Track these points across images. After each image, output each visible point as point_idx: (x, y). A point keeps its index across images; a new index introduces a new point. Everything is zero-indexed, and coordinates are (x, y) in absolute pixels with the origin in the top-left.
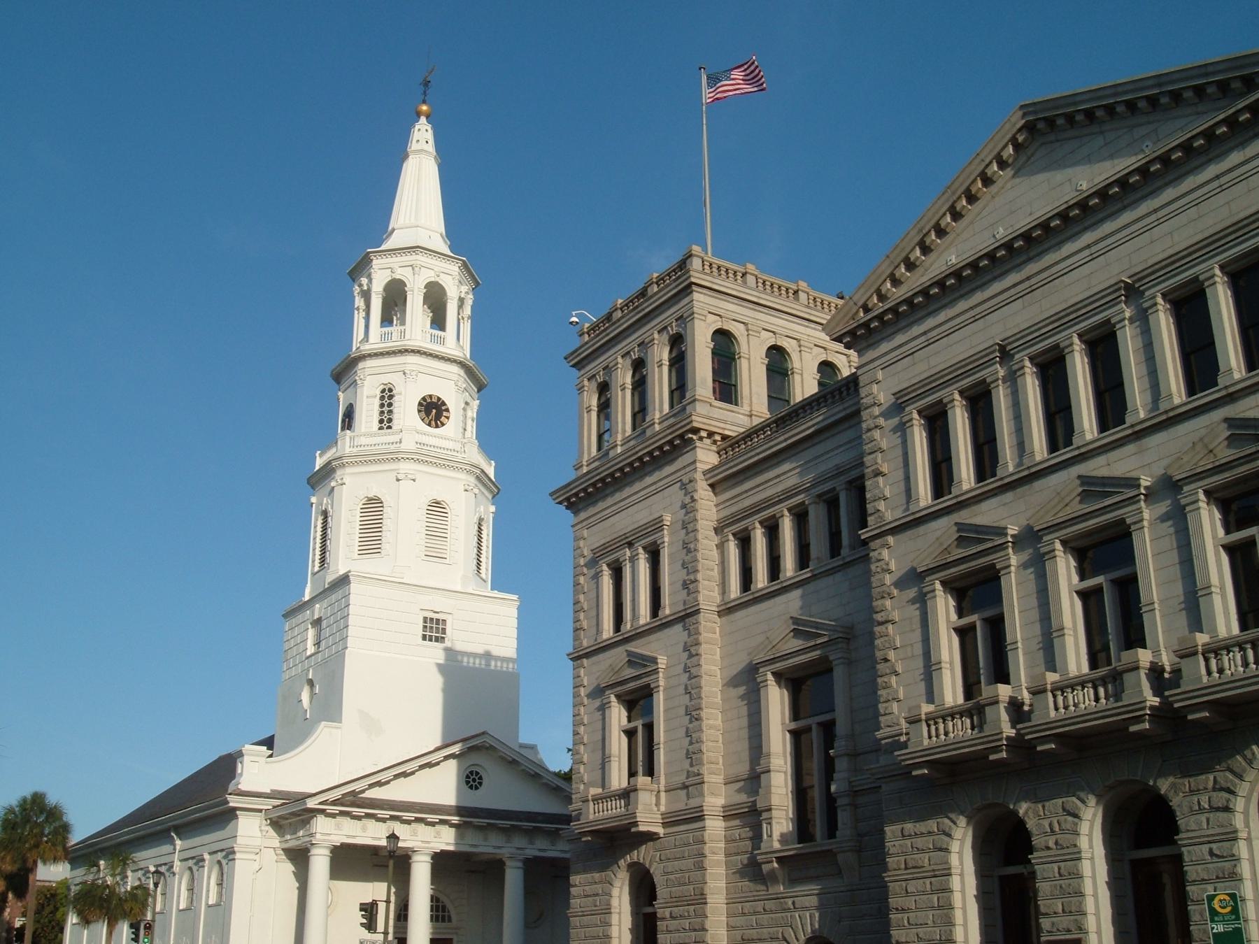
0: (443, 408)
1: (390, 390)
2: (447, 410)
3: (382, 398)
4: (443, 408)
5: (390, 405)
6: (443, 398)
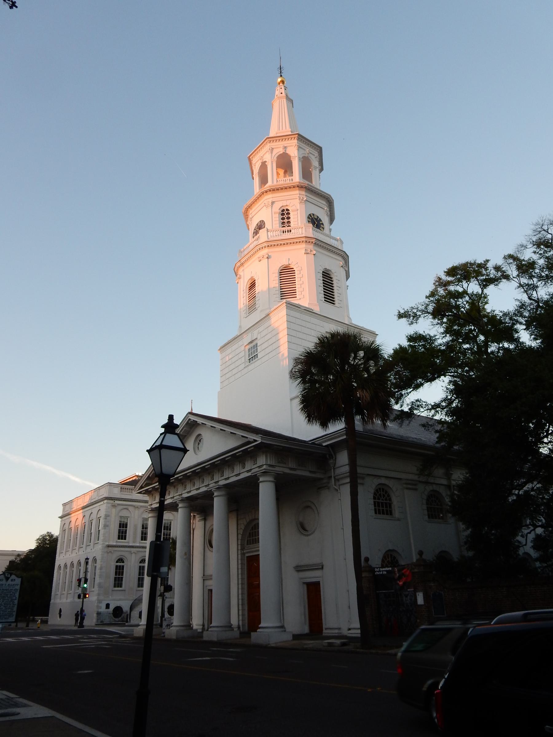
0: (321, 222)
1: (287, 210)
2: (323, 224)
3: (283, 214)
4: (321, 222)
5: (288, 218)
6: (320, 217)
